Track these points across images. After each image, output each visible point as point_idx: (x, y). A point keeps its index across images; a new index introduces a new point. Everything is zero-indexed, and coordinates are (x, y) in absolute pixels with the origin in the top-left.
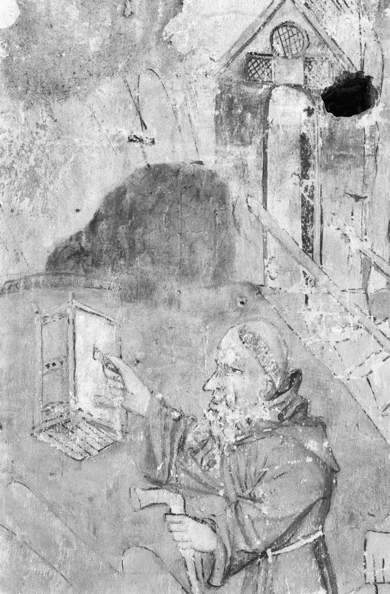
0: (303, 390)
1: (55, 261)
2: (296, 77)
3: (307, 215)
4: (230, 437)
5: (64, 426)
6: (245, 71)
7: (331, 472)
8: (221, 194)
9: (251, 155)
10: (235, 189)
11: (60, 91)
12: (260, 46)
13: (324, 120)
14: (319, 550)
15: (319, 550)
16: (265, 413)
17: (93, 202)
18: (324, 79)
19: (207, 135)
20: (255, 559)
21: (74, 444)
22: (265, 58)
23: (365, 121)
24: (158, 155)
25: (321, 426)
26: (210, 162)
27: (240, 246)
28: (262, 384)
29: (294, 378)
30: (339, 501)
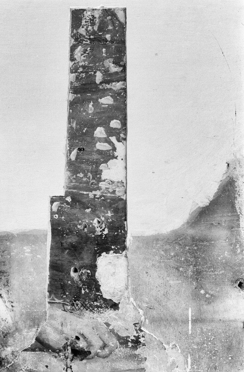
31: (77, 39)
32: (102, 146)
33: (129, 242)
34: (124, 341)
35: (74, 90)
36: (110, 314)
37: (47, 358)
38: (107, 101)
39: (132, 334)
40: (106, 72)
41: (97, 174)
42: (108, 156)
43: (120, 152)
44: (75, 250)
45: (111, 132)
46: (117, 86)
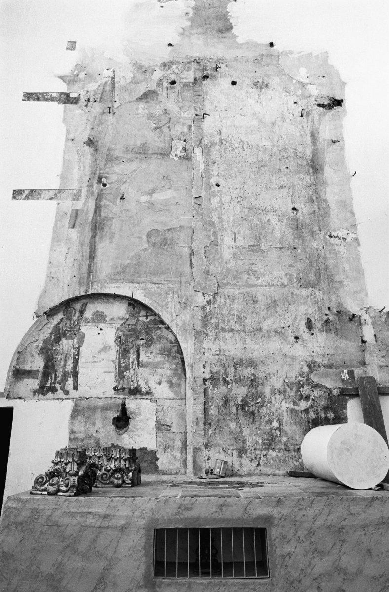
0: (167, 111)
1: (137, 99)
2: (166, 81)
3: (168, 94)
4: (158, 115)
5: (138, 114)
6: (160, 81)
7: (170, 119)
8: (157, 93)
9: (161, 89)
10: (159, 92)
11: (138, 83)
12: (162, 78)
13: (170, 85)
14: (169, 127)
15: (169, 127)
16: (162, 113)
17: (142, 93)
18: (170, 81)
19: (156, 87)
20: (160, 127)
21: (139, 116)
22: (163, 80)
23: (175, 85)
24: (149, 89)
25: (169, 114)
26: (156, 89)
27: (159, 97)
28: (161, 110)
29: (166, 110)
30: (171, 121)
31: (28, 100)
32: (49, 97)
33: (68, 92)
34: (87, 93)
35: (38, 101)
36: (82, 96)
37: (89, 105)
38: (41, 96)
39: (86, 92)
40: (35, 96)
41: (54, 97)
42: (51, 96)
43: (51, 94)
44: (68, 101)
45: (47, 95)
46: (38, 94)
